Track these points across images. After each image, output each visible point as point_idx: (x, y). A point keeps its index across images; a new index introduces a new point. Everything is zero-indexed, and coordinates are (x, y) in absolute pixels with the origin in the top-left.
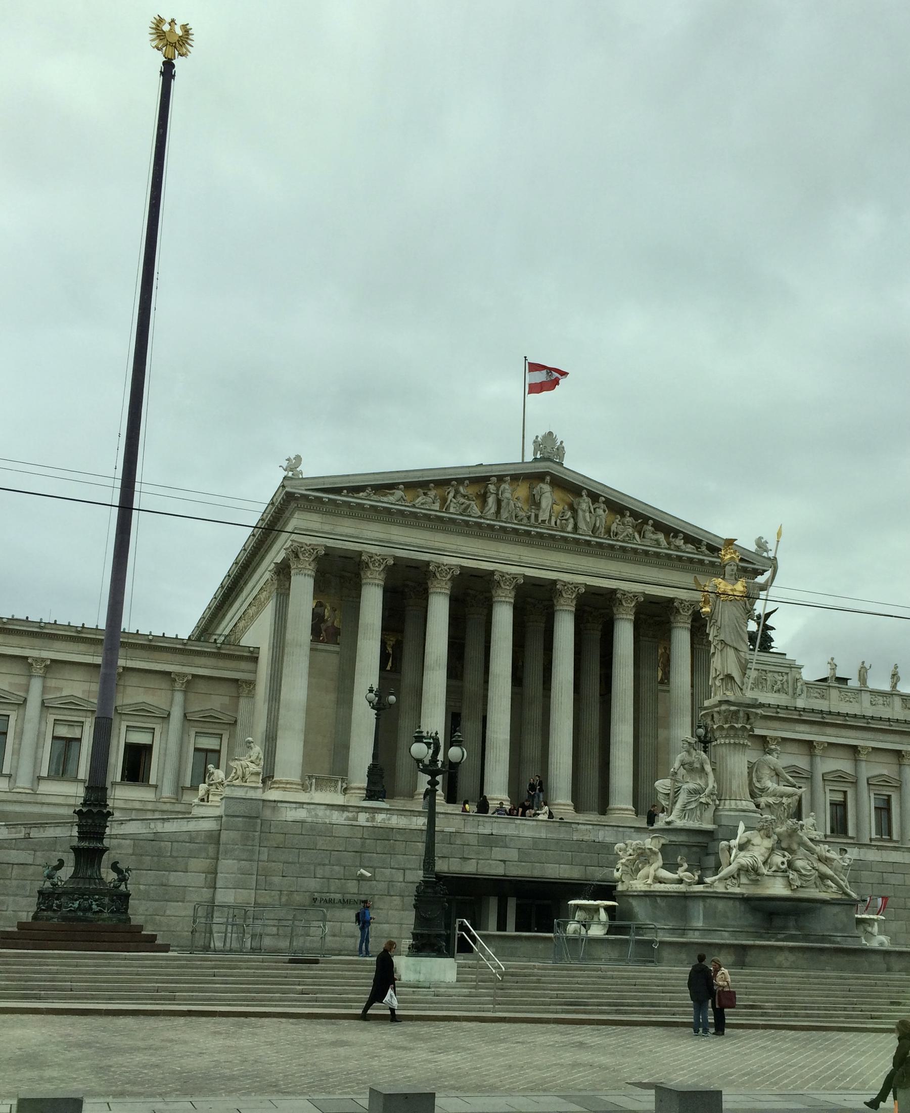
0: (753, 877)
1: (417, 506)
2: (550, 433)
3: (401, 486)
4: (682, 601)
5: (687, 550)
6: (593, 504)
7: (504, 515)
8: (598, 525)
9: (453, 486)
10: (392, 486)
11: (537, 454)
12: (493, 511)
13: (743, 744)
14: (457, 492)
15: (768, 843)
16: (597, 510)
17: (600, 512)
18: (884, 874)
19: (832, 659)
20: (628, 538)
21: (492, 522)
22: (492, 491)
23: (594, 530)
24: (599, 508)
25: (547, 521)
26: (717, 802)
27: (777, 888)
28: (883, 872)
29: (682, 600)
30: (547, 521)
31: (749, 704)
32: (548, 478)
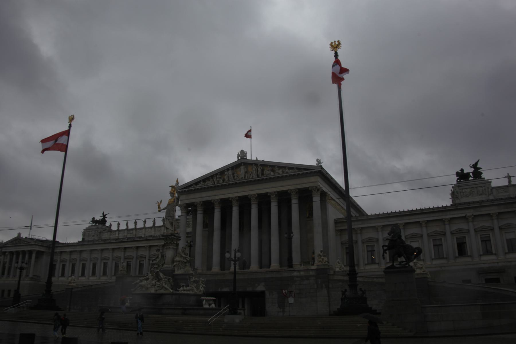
1: (205, 185)
2: (242, 150)
3: (202, 181)
4: (291, 190)
5: (290, 172)
6: (257, 167)
7: (230, 180)
8: (258, 173)
11: (239, 158)
14: (217, 178)
17: (259, 169)
19: (508, 174)
21: (226, 183)
22: (226, 174)
23: (258, 176)
24: (258, 168)
25: (243, 178)
29: (291, 189)
30: (243, 178)
32: (242, 164)
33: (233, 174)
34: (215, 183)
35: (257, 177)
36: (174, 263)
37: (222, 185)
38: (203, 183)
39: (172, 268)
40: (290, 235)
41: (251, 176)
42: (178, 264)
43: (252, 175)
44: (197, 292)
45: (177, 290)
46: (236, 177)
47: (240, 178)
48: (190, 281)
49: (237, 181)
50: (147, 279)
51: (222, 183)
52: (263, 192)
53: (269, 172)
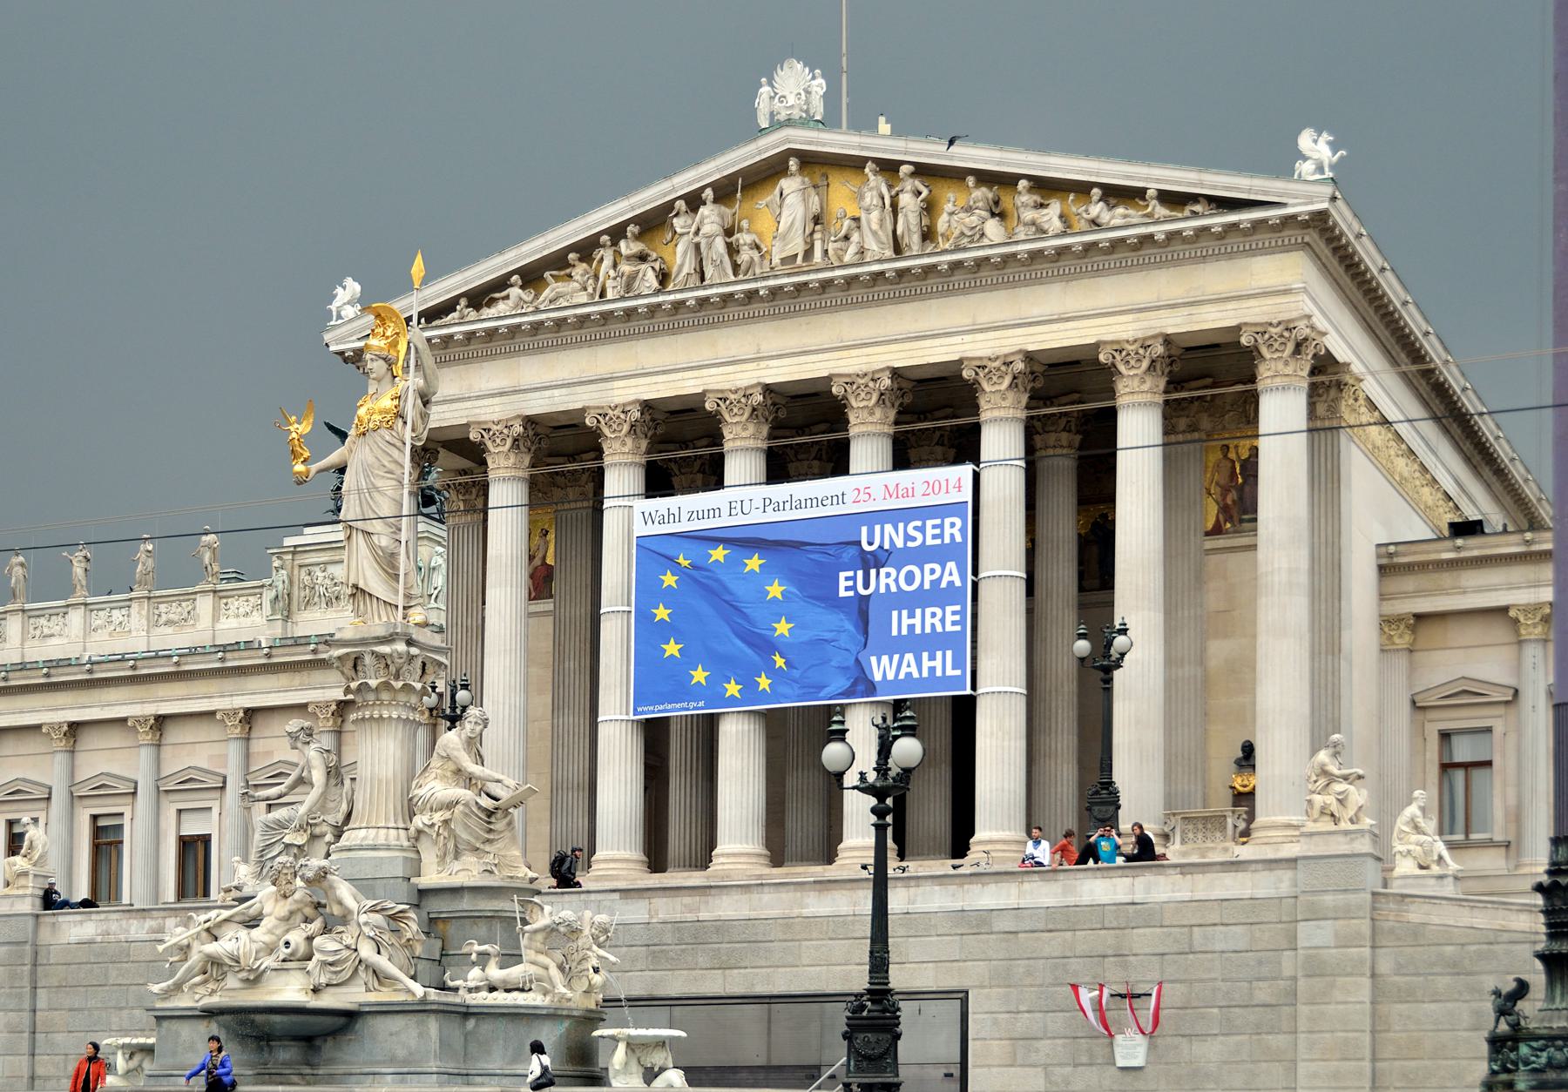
0: (243, 975)
7: (709, 271)
9: (604, 246)
10: (501, 284)
12: (689, 266)
13: (372, 717)
15: (283, 908)
16: (901, 196)
17: (906, 200)
18: (1195, 929)
20: (966, 240)
21: (679, 296)
22: (679, 230)
23: (898, 249)
25: (800, 258)
26: (329, 838)
27: (289, 990)
28: (1191, 926)
29: (1118, 342)
30: (800, 258)
31: (378, 638)
33: (729, 232)
34: (602, 295)
35: (889, 253)
36: (412, 815)
37: (654, 309)
38: (527, 296)
39: (402, 849)
40: (1110, 644)
41: (852, 249)
42: (446, 822)
43: (855, 237)
44: (569, 994)
45: (443, 987)
46: (744, 256)
47: (776, 261)
48: (527, 928)
49: (755, 280)
50: (252, 923)
51: (657, 292)
52: (932, 360)
53: (973, 220)
